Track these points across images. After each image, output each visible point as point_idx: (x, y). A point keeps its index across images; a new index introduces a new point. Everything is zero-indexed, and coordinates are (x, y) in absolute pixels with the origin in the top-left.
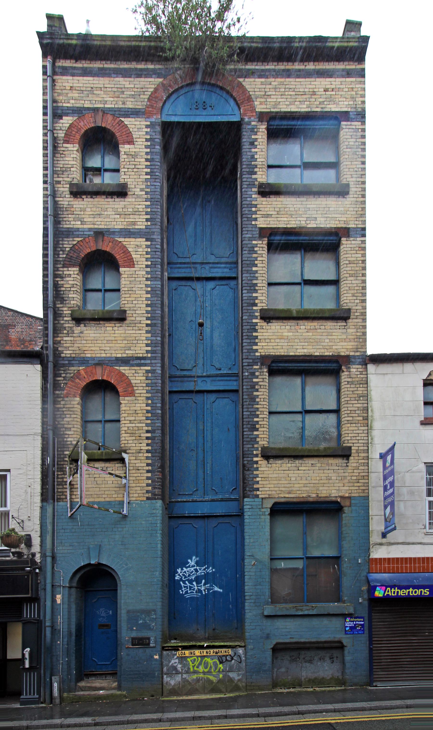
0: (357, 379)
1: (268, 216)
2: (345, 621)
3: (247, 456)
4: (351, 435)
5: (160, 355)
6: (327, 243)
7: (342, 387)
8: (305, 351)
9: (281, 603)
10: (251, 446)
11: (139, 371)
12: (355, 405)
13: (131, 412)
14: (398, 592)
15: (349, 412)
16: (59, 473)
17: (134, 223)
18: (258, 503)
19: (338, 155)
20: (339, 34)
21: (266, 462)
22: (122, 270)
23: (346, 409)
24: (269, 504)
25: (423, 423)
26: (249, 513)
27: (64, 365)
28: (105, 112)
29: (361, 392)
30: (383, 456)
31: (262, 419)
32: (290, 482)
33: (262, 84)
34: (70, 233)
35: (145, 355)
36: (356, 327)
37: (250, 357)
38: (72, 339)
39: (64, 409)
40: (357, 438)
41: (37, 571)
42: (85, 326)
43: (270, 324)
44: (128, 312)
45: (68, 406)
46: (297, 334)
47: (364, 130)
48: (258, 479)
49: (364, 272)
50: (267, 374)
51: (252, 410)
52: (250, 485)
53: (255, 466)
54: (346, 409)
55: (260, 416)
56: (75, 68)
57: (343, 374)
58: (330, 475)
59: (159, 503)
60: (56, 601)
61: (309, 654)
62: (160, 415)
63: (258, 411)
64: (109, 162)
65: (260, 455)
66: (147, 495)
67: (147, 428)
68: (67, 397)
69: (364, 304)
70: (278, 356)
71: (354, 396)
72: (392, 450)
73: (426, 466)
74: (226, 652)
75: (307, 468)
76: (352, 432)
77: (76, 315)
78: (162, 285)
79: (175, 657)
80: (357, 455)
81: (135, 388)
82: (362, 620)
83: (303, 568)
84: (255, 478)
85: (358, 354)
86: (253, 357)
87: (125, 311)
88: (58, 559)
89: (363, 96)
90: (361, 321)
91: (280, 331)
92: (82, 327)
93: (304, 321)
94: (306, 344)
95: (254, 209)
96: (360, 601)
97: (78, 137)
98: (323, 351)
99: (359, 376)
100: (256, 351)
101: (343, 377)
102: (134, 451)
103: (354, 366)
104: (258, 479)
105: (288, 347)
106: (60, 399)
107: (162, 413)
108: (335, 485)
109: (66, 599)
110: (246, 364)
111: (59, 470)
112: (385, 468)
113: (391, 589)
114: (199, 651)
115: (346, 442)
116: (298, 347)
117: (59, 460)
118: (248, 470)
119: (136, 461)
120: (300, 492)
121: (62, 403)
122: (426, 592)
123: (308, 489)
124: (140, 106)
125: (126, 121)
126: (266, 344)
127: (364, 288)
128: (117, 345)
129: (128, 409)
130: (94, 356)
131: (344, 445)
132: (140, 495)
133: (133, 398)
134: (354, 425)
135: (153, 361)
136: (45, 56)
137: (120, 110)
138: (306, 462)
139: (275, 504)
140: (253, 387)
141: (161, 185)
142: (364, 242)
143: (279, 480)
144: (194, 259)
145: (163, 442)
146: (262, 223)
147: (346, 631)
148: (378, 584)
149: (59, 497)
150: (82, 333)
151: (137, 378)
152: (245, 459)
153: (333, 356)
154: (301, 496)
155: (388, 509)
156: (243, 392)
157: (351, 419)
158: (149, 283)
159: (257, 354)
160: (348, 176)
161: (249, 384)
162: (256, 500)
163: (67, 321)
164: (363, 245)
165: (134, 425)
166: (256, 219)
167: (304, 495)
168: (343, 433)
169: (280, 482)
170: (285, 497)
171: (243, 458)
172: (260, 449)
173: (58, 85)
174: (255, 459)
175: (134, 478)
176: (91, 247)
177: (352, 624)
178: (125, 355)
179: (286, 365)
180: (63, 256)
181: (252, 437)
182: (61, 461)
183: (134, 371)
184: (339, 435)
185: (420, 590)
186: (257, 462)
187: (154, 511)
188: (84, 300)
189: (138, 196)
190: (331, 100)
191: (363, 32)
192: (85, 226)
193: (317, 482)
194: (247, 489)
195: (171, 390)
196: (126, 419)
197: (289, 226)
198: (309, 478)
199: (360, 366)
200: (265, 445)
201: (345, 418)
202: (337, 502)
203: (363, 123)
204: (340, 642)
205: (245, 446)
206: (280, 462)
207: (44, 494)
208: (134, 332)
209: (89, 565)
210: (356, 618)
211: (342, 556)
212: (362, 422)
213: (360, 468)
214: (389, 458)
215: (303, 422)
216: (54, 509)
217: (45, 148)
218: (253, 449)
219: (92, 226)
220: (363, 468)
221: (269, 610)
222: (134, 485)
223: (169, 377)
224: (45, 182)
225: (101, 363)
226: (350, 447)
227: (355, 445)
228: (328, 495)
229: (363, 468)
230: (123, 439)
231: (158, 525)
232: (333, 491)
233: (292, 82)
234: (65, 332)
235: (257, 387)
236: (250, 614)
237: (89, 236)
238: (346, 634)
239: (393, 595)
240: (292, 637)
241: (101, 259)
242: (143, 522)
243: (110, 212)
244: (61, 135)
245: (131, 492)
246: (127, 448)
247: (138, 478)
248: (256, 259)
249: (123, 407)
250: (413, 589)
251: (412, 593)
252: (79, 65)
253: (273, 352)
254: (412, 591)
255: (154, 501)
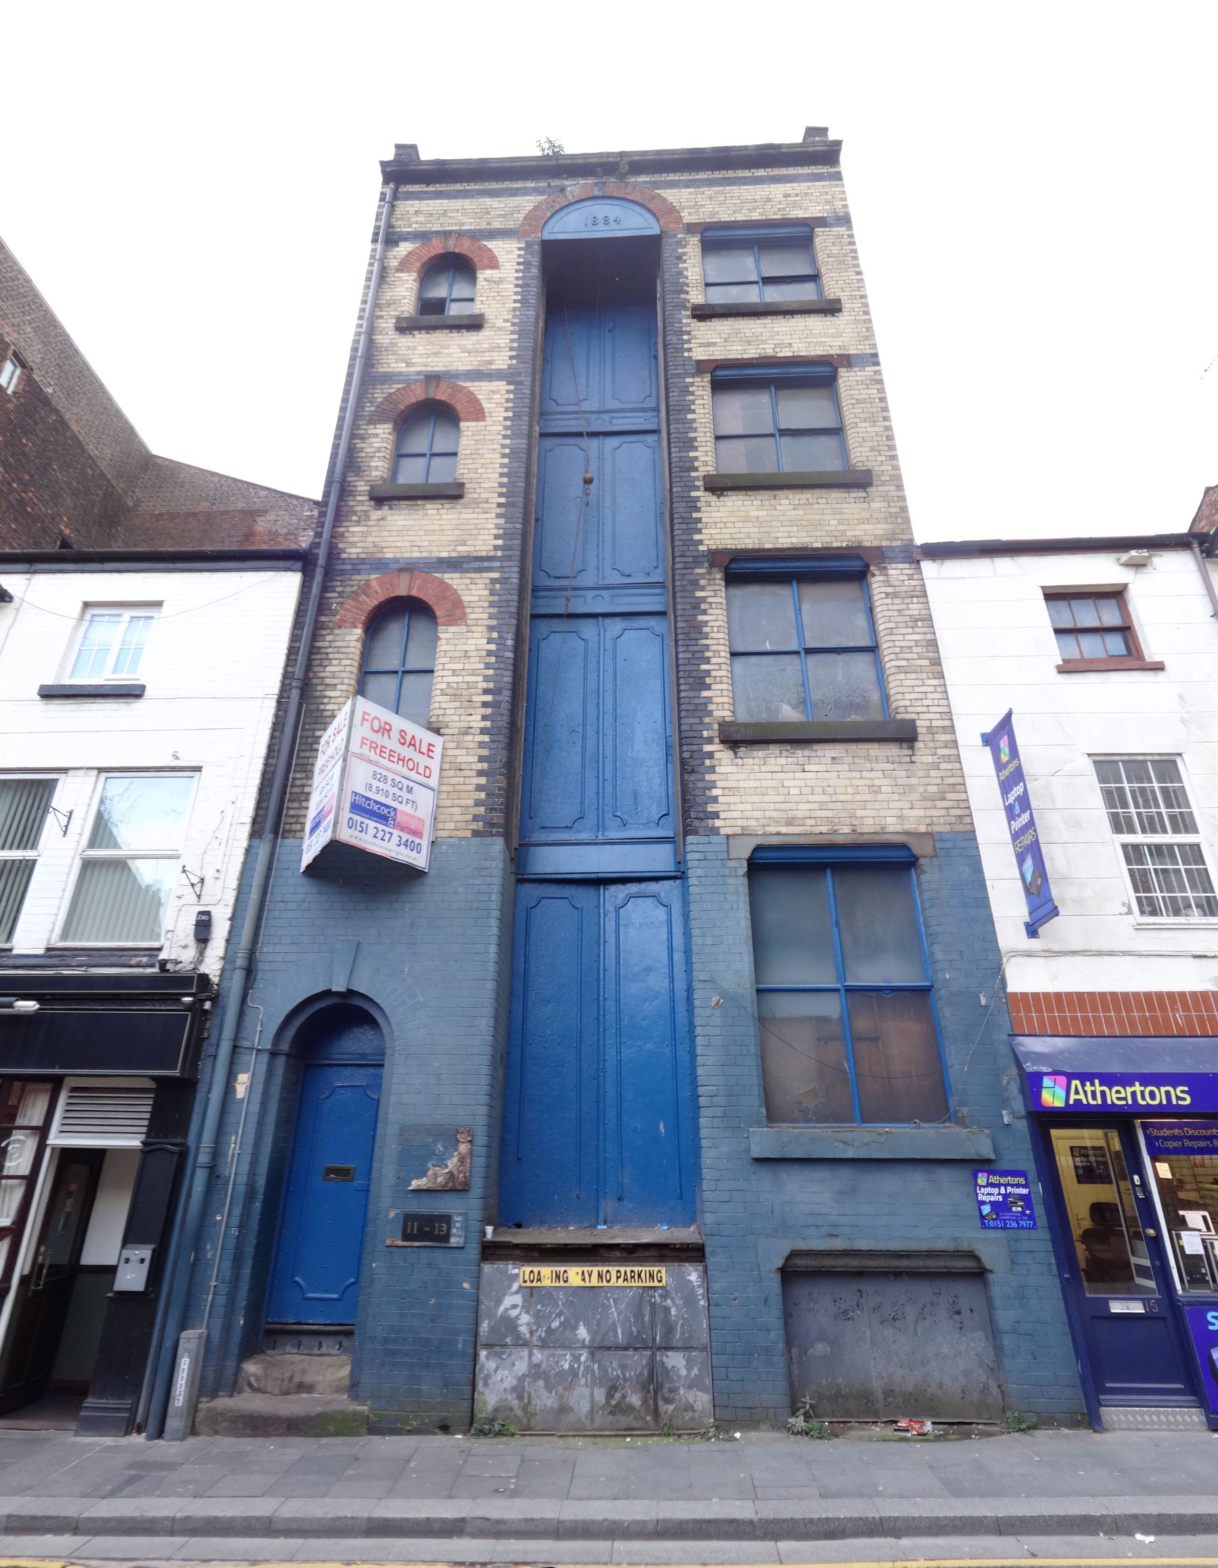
0: (904, 589)
1: (709, 344)
2: (976, 1184)
3: (689, 741)
4: (908, 696)
5: (518, 553)
6: (817, 376)
7: (877, 604)
8: (794, 540)
9: (794, 1121)
10: (697, 720)
11: (478, 581)
12: (907, 637)
13: (456, 654)
14: (1103, 1093)
15: (898, 650)
16: (298, 776)
17: (491, 363)
18: (717, 848)
19: (813, 260)
20: (800, 140)
21: (731, 753)
22: (463, 425)
23: (891, 644)
24: (744, 850)
25: (1061, 670)
26: (699, 872)
27: (343, 572)
28: (460, 234)
29: (916, 612)
30: (989, 740)
31: (717, 667)
32: (788, 798)
33: (690, 193)
34: (388, 378)
35: (492, 554)
36: (886, 498)
37: (688, 554)
38: (365, 529)
39: (330, 650)
40: (925, 702)
41: (207, 1005)
42: (391, 509)
43: (722, 498)
44: (467, 486)
45: (338, 644)
46: (775, 512)
47: (851, 236)
48: (715, 792)
49: (885, 414)
50: (723, 583)
51: (695, 648)
52: (699, 805)
53: (707, 762)
54: (891, 644)
55: (713, 660)
56: (427, 192)
57: (873, 580)
58: (877, 782)
59: (498, 845)
60: (234, 1091)
61: (893, 1294)
62: (511, 661)
63: (708, 650)
64: (460, 290)
65: (717, 740)
66: (474, 826)
67: (485, 685)
68: (340, 627)
69: (895, 462)
70: (742, 550)
71: (904, 619)
72: (1006, 724)
73: (1095, 762)
74: (651, 1276)
75: (823, 768)
76: (910, 690)
77: (381, 493)
78: (530, 445)
79: (515, 1287)
80: (929, 737)
81: (468, 610)
82: (1022, 1181)
83: (841, 1018)
84: (709, 789)
85: (898, 543)
86: (695, 554)
87: (462, 485)
88: (259, 977)
89: (845, 199)
90: (893, 488)
91: (743, 509)
92: (385, 511)
93: (786, 492)
94: (795, 529)
95: (685, 337)
96: (1006, 1120)
97: (418, 265)
98: (828, 539)
99: (906, 583)
100: (701, 542)
101: (874, 586)
102: (456, 731)
103: (893, 566)
104: (715, 792)
105: (759, 536)
106: (324, 632)
107: (516, 659)
108: (892, 805)
109: (259, 1088)
110: (681, 566)
111: (298, 768)
112: (999, 766)
113: (1083, 1085)
114: (579, 1269)
115: (902, 710)
116: (779, 535)
117: (303, 747)
118: (693, 771)
119: (458, 752)
120: (812, 822)
121: (329, 638)
122: (1181, 1096)
123: (830, 814)
124: (510, 225)
125: (490, 244)
126: (718, 531)
127: (890, 438)
128: (443, 538)
129: (452, 648)
130: (398, 555)
131: (899, 717)
132: (459, 825)
133: (464, 629)
134: (913, 676)
135: (505, 564)
136: (386, 182)
137: (481, 231)
138: (820, 753)
139: (758, 849)
140: (696, 606)
141: (534, 312)
142: (878, 372)
143: (763, 794)
144: (586, 406)
145: (513, 713)
146: (699, 354)
147: (983, 1217)
148: (1044, 1069)
149: (287, 827)
150: (383, 519)
151: (474, 592)
152: (685, 748)
153: (848, 548)
154: (817, 830)
155: (1029, 865)
156: (675, 617)
157: (904, 663)
158: (508, 441)
159: (701, 548)
160: (833, 286)
161: (689, 600)
162: (714, 839)
163: (360, 502)
164: (877, 377)
165: (460, 679)
166: (690, 350)
167: (824, 829)
168: (892, 692)
169: (766, 799)
170: (778, 834)
171: (681, 745)
172: (716, 726)
173: (398, 211)
174: (707, 748)
175: (450, 788)
176: (418, 394)
177: (995, 1195)
178: (454, 554)
179: (759, 565)
180: (369, 408)
181: (697, 701)
182: (305, 751)
183: (468, 581)
184: (885, 698)
185: (1163, 1089)
186: (710, 755)
187: (488, 864)
188: (394, 470)
189: (500, 329)
190: (795, 205)
191: (832, 136)
192: (412, 369)
193: (849, 797)
194: (693, 814)
195: (535, 612)
196: (447, 666)
197: (745, 356)
198: (830, 790)
199: (907, 566)
200: (727, 719)
201: (890, 663)
202: (904, 847)
203: (850, 228)
204: (972, 1255)
205: (683, 721)
206: (761, 754)
207: (259, 820)
208: (475, 516)
209: (328, 993)
210: (1004, 1174)
211: (936, 986)
212: (928, 669)
213: (943, 766)
214: (1004, 744)
215: (804, 671)
216: (272, 854)
217: (368, 279)
218: (700, 728)
219: (423, 369)
220: (949, 766)
221: (764, 1140)
222: (448, 803)
223: (533, 591)
224: (360, 318)
225: (408, 568)
226: (914, 721)
227: (922, 716)
228: (878, 829)
229: (949, 766)
230: (436, 705)
231: (494, 897)
232: (890, 820)
233: (735, 190)
234: (355, 518)
235: (703, 606)
236: (713, 1152)
237: (416, 381)
238: (985, 1226)
239: (1092, 1102)
240: (833, 1231)
241: (432, 410)
242: (461, 890)
243: (454, 350)
244: (394, 263)
245: (441, 818)
246: (441, 725)
247: (458, 788)
248: (693, 402)
249: (442, 646)
250: (1144, 1083)
251: (1143, 1098)
252: (431, 188)
253: (731, 544)
254: (1142, 1093)
255: (488, 840)
